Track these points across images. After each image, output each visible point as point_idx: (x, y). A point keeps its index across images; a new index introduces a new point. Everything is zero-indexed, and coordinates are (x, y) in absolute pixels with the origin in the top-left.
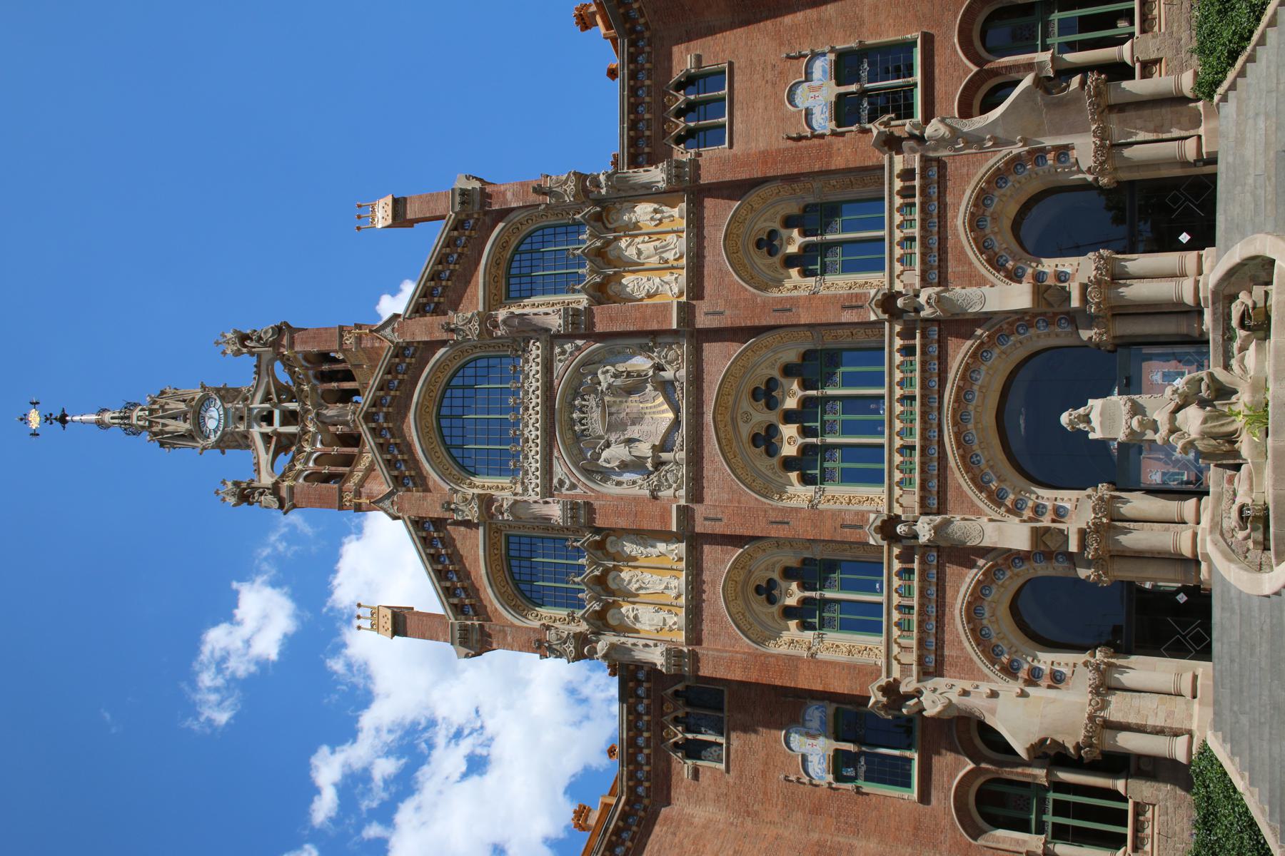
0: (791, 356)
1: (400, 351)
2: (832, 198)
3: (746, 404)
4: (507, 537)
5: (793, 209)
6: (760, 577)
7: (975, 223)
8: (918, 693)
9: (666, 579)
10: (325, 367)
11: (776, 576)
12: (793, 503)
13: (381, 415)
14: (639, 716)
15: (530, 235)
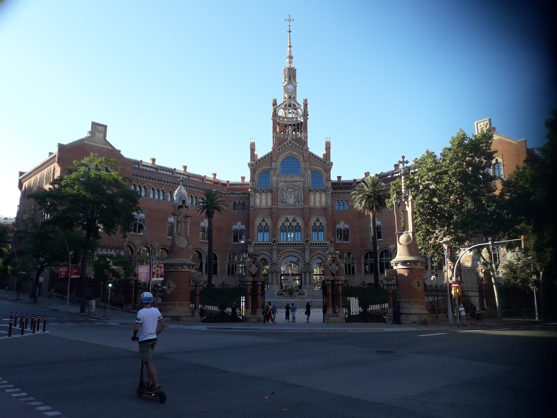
0: (300, 224)
1: (302, 149)
2: (324, 231)
3: (293, 217)
4: (270, 172)
5: (323, 224)
6: (266, 219)
7: (319, 253)
8: (251, 246)
9: (264, 203)
10: (300, 127)
11: (266, 222)
12: (278, 226)
13: (290, 145)
14: (239, 195)
15: (322, 176)
